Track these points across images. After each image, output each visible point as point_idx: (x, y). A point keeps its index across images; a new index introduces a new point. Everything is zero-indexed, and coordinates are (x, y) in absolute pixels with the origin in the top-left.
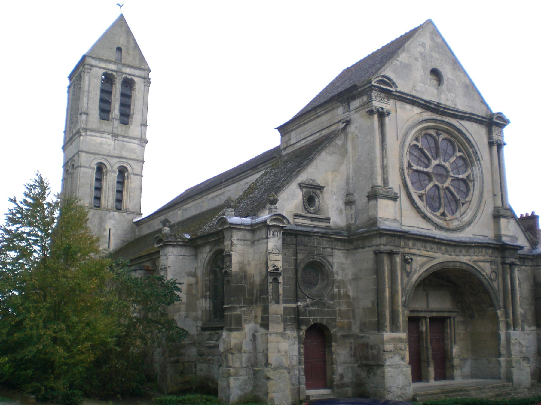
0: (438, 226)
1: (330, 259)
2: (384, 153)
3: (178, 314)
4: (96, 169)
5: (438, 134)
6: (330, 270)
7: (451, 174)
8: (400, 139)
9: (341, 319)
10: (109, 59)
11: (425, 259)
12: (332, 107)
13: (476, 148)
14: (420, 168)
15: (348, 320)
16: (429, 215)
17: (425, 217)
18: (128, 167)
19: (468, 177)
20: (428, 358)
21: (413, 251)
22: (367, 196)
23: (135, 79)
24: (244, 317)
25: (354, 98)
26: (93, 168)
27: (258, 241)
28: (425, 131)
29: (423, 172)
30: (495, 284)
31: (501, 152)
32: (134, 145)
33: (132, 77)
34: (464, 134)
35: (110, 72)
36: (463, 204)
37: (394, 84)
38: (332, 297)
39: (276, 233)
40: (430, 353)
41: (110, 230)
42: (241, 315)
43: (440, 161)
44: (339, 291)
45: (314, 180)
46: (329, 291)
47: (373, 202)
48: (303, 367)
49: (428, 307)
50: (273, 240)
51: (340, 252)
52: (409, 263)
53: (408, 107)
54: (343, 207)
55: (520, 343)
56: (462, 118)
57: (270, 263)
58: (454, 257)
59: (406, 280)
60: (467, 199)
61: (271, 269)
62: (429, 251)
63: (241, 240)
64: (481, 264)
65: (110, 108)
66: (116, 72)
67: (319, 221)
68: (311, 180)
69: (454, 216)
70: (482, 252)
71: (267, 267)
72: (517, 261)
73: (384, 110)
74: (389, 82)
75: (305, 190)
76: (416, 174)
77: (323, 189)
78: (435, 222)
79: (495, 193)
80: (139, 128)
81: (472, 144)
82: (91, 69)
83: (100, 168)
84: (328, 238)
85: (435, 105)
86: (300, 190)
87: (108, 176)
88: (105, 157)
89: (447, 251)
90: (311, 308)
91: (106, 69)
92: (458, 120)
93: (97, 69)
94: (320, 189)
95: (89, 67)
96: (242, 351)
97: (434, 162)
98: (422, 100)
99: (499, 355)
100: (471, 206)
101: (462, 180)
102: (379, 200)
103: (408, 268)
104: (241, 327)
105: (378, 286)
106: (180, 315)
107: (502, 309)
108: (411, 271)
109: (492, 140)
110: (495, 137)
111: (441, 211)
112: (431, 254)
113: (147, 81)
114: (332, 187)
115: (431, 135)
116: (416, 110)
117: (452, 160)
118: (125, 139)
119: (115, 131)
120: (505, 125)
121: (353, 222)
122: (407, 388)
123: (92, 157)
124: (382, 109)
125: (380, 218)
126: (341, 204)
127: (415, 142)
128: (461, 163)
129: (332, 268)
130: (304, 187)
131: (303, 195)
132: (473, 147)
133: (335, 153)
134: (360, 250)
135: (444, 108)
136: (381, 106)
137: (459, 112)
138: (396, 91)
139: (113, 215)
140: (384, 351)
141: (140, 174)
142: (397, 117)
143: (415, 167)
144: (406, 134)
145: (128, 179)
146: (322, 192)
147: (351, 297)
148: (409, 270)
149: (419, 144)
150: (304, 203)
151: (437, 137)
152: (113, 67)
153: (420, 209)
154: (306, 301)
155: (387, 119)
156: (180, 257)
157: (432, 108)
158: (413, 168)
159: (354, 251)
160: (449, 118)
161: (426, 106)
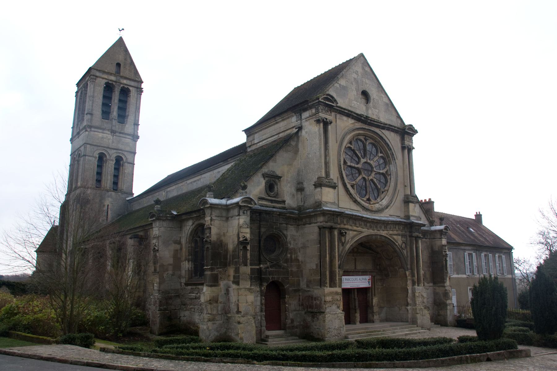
0: (365, 208)
1: (285, 232)
2: (327, 153)
3: (166, 273)
4: (98, 158)
5: (366, 140)
6: (284, 240)
7: (375, 169)
8: (338, 142)
9: (292, 277)
10: (111, 72)
11: (355, 233)
12: (287, 117)
13: (393, 151)
14: (353, 165)
15: (297, 278)
16: (359, 200)
17: (355, 201)
18: (123, 157)
19: (386, 172)
20: (355, 307)
21: (346, 227)
22: (314, 185)
23: (131, 88)
24: (219, 276)
25: (305, 110)
26: (95, 157)
27: (232, 217)
28: (357, 137)
29: (354, 168)
30: (405, 252)
31: (410, 154)
32: (128, 140)
33: (128, 86)
34: (384, 140)
35: (111, 82)
36: (383, 192)
37: (335, 101)
38: (286, 261)
39: (245, 212)
40: (357, 303)
41: (108, 205)
42: (217, 274)
43: (367, 160)
44: (291, 256)
45: (274, 172)
46: (283, 256)
47: (318, 189)
48: (264, 313)
49: (355, 268)
50: (243, 217)
51: (292, 226)
52: (343, 236)
53: (345, 118)
54: (294, 192)
55: (422, 295)
56: (383, 128)
57: (241, 235)
58: (376, 231)
59: (341, 248)
60: (386, 189)
61: (241, 239)
62: (358, 227)
63: (218, 216)
64: (395, 237)
65: (110, 110)
66: (116, 82)
67: (278, 203)
68: (272, 171)
69: (376, 201)
70: (396, 228)
71: (239, 238)
72: (420, 235)
73: (328, 120)
74: (332, 99)
75: (267, 179)
76: (350, 169)
77: (280, 179)
78: (363, 205)
79: (406, 184)
80: (133, 127)
81: (390, 148)
82: (95, 79)
83: (101, 158)
84: (284, 215)
85: (364, 118)
86: (263, 179)
87: (107, 163)
88: (105, 149)
89: (371, 227)
90: (270, 269)
91: (108, 80)
92: (380, 130)
93: (101, 79)
94: (278, 179)
95: (94, 77)
96: (219, 302)
97: (363, 160)
98: (355, 113)
99: (407, 304)
100: (388, 194)
101: (383, 174)
102: (323, 187)
103: (343, 239)
104: (218, 283)
105: (320, 253)
106: (168, 274)
107: (409, 270)
108: (345, 241)
109: (404, 145)
110: (406, 143)
111: (367, 197)
112: (359, 229)
113: (140, 91)
114: (287, 177)
115: (361, 140)
116: (351, 121)
117: (375, 159)
118: (121, 135)
119: (114, 128)
120: (413, 135)
121: (302, 204)
122: (342, 329)
123: (96, 148)
124: (326, 119)
125: (323, 202)
126: (293, 190)
127: (349, 145)
128: (382, 161)
129: (286, 239)
130: (266, 176)
131: (266, 183)
132: (391, 149)
133: (290, 151)
134: (308, 226)
135: (371, 120)
136: (325, 117)
137: (381, 123)
138: (337, 106)
139: (111, 194)
140: (325, 301)
141: (132, 162)
142: (336, 126)
143: (349, 164)
144: (343, 139)
145: (123, 166)
146: (280, 181)
147: (300, 261)
148: (343, 241)
149: (352, 147)
150: (266, 189)
151: (365, 142)
152: (113, 78)
153: (352, 195)
154: (267, 264)
155: (330, 127)
156: (169, 229)
157: (362, 120)
158: (347, 164)
159: (303, 226)
160: (374, 128)
161: (358, 118)
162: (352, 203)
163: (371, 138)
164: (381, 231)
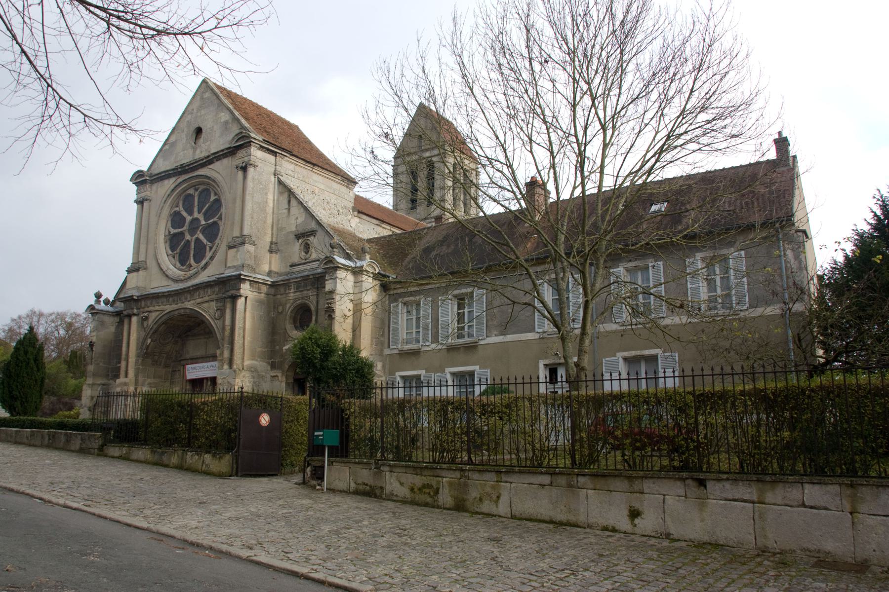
7: (203, 222)
11: (158, 313)
53: (166, 182)
56: (210, 162)
64: (205, 305)
89: (174, 301)
92: (209, 167)
112: (162, 307)
116: (172, 180)
135: (188, 166)
137: (202, 160)
143: (173, 231)
155: (146, 204)
162: (165, 278)
163: (201, 184)
164: (186, 303)
